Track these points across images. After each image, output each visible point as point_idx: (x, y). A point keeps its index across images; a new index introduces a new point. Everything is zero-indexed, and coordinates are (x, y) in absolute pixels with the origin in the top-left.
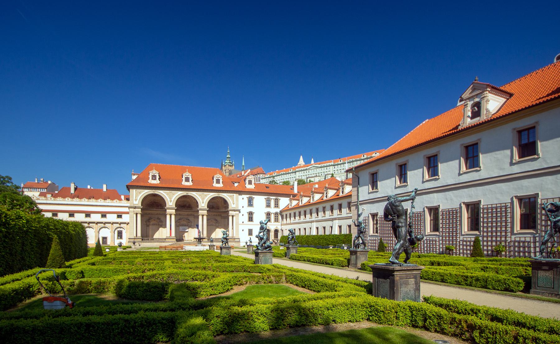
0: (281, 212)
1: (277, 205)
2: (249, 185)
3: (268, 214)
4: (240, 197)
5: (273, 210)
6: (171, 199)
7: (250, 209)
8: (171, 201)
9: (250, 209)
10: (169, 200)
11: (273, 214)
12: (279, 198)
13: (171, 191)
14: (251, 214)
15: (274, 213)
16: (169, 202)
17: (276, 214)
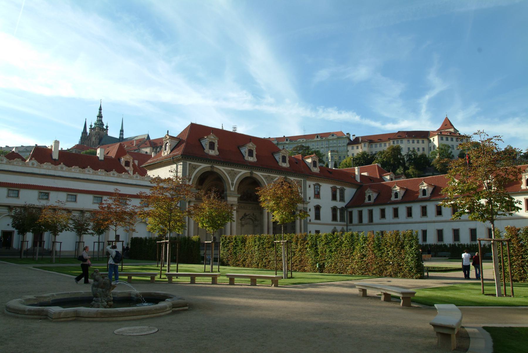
0: (347, 207)
1: (342, 199)
2: (314, 168)
3: (334, 209)
4: (308, 183)
5: (340, 205)
6: (233, 181)
7: (316, 202)
8: (232, 184)
9: (316, 202)
10: (230, 182)
11: (338, 210)
12: (345, 188)
13: (233, 169)
14: (318, 208)
15: (339, 208)
16: (231, 186)
17: (342, 210)
